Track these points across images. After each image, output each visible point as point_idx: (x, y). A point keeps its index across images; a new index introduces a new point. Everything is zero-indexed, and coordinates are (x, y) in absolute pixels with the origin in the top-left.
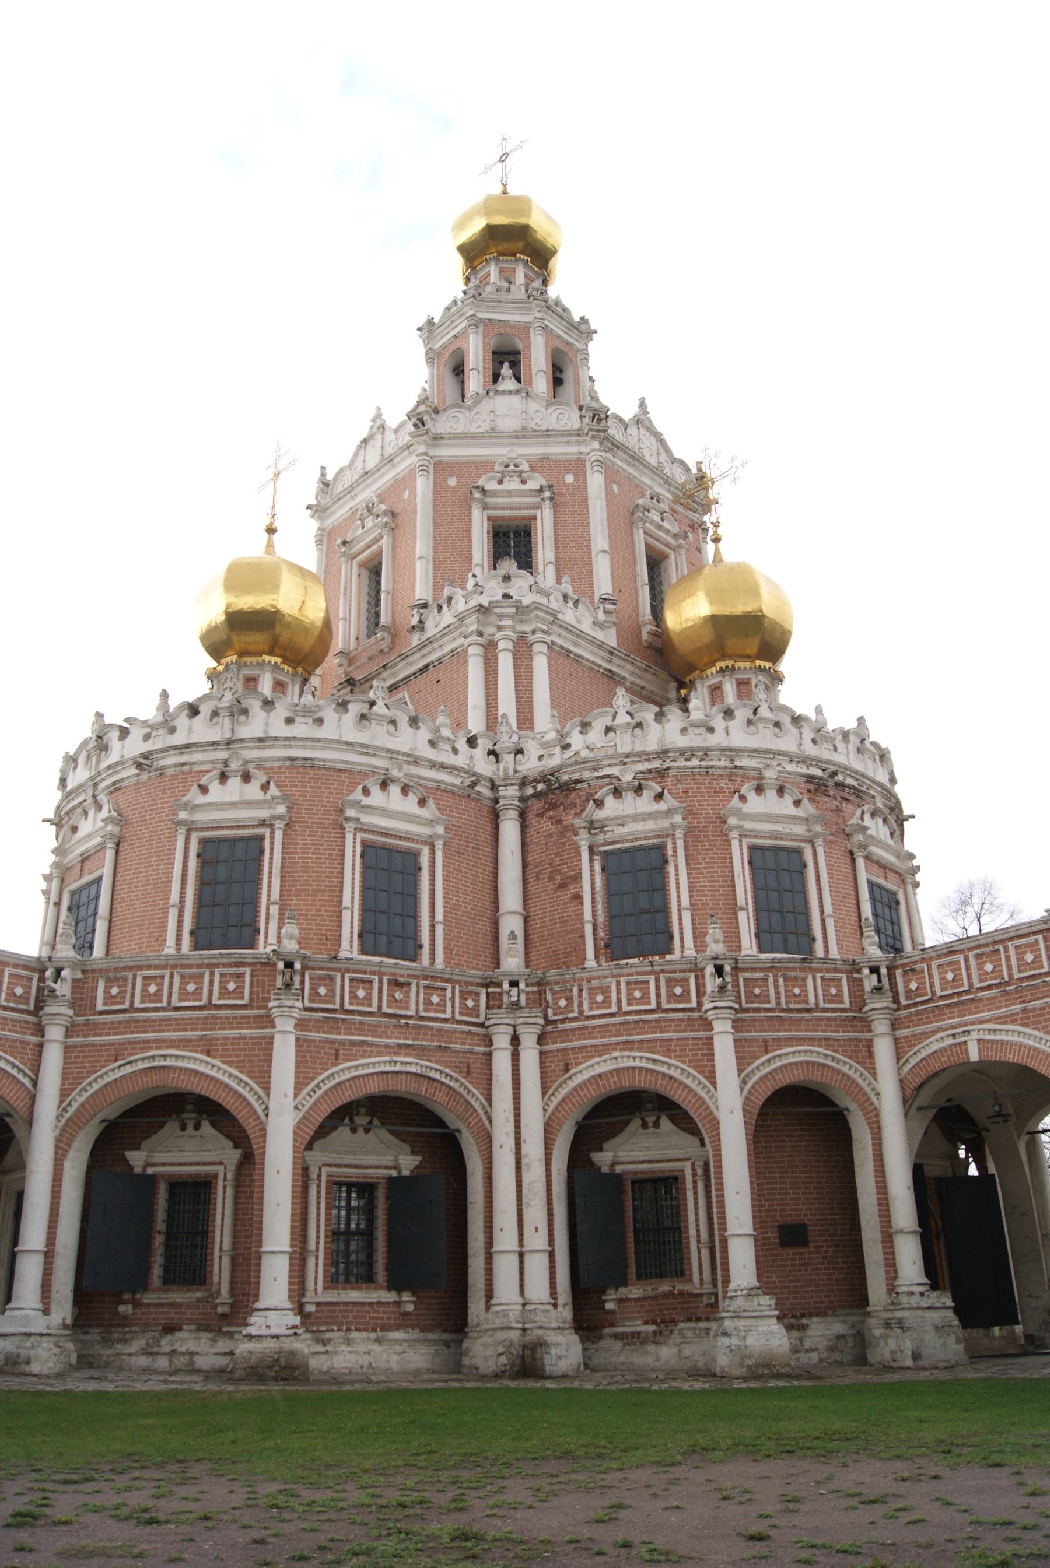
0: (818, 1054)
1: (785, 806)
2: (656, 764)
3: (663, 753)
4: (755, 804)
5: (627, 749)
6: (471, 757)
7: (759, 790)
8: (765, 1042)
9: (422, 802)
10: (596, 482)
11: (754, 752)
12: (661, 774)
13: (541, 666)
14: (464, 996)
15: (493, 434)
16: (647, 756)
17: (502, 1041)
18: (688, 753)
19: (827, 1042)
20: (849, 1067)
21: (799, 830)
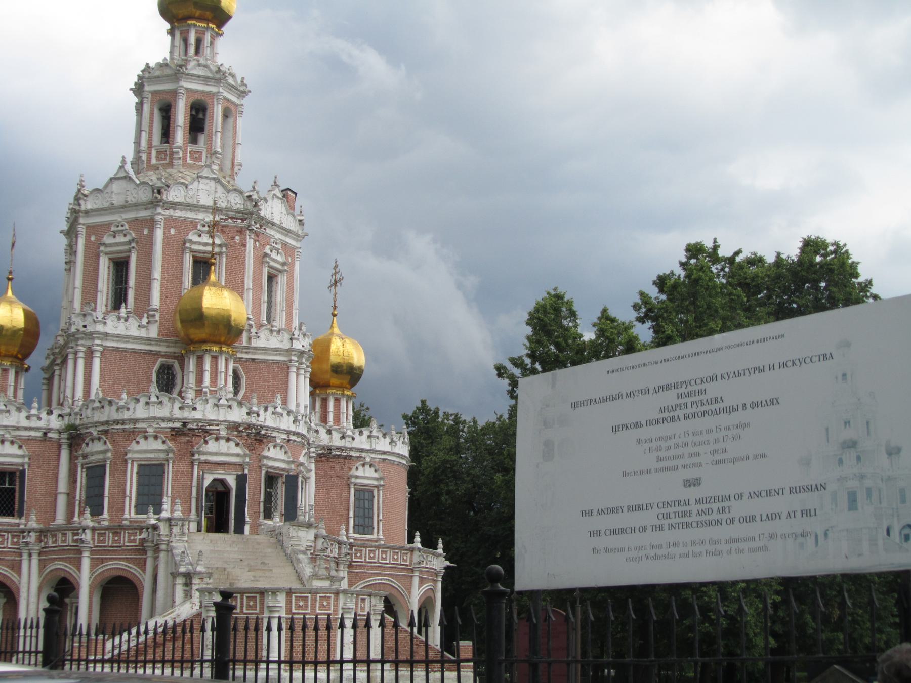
0: (122, 564)
1: (158, 445)
2: (105, 428)
3: (107, 423)
4: (144, 445)
5: (95, 420)
6: (48, 421)
7: (146, 438)
8: (102, 559)
9: (20, 447)
10: (159, 234)
11: (143, 420)
12: (106, 432)
13: (97, 363)
14: (13, 537)
15: (112, 209)
16: (103, 424)
17: (25, 556)
18: (117, 422)
19: (127, 559)
20: (134, 570)
21: (162, 456)
